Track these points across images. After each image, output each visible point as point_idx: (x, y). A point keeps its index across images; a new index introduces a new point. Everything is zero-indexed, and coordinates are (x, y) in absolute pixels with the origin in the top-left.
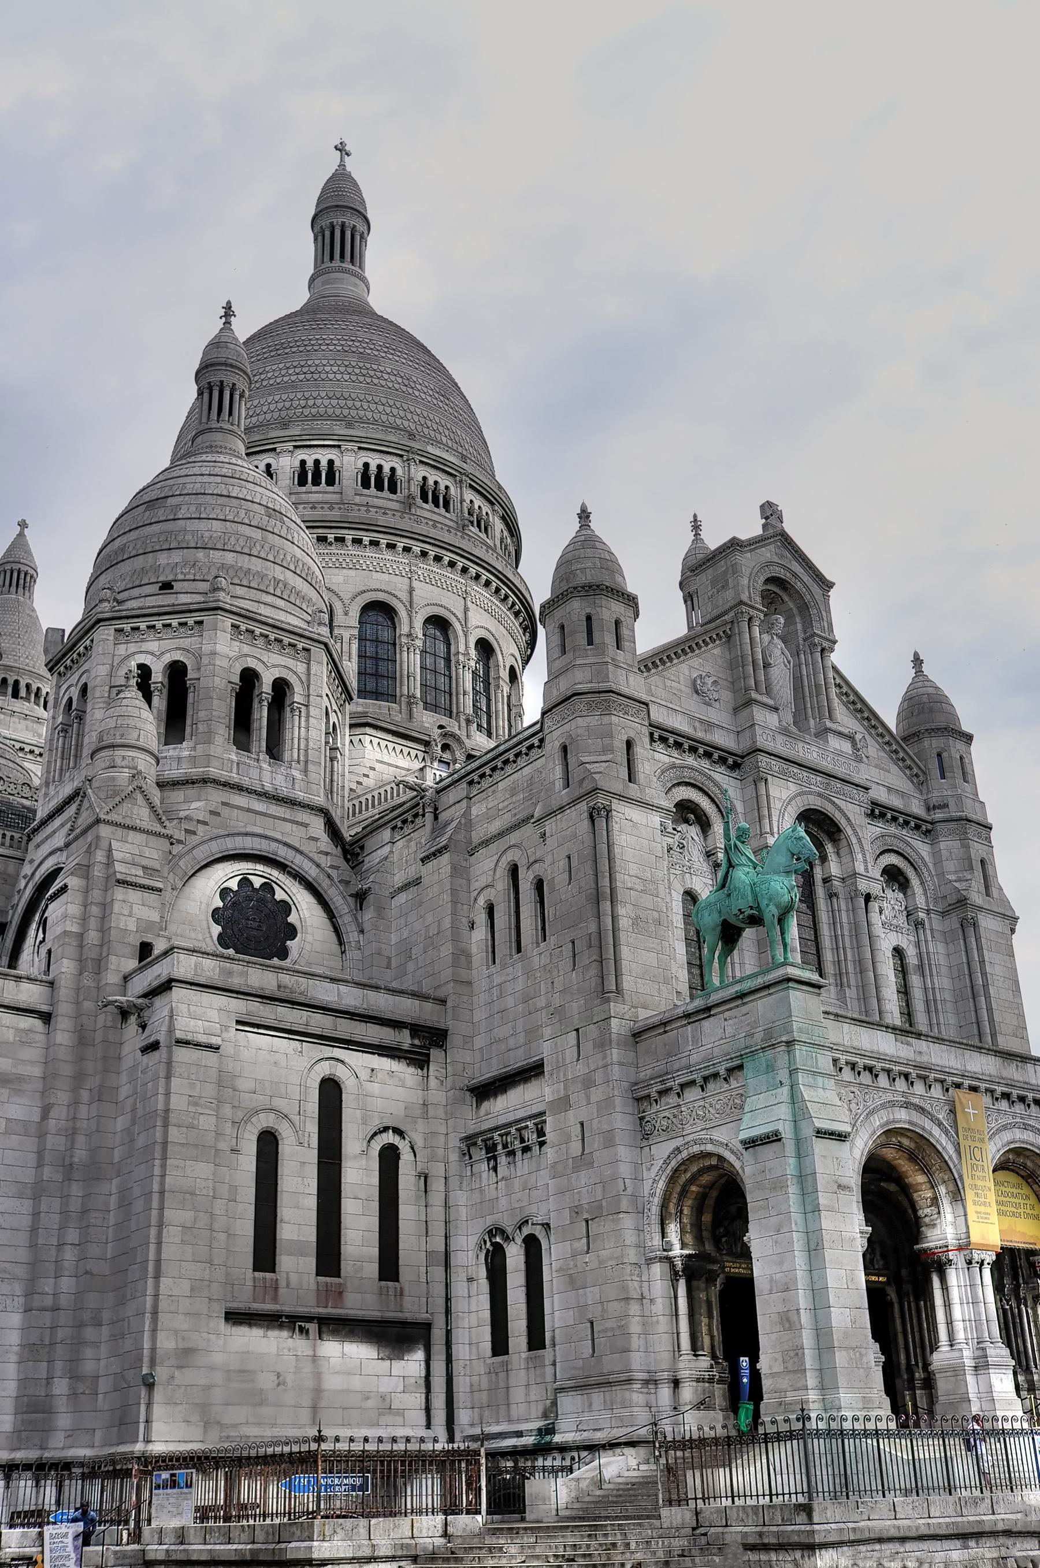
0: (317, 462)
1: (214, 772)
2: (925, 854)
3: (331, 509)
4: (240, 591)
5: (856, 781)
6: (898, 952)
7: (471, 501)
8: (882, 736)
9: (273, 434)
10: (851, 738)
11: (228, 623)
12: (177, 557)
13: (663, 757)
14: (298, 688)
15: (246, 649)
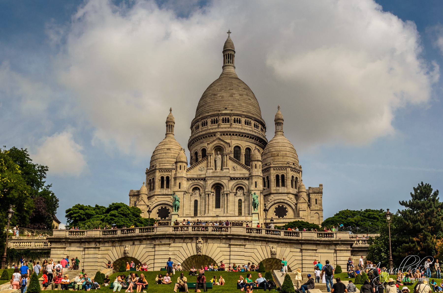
0: (204, 121)
1: (156, 193)
2: (246, 183)
3: (204, 131)
4: (162, 165)
5: (227, 176)
6: (240, 200)
7: (235, 118)
8: (241, 165)
9: (198, 118)
10: (229, 169)
11: (158, 171)
12: (154, 161)
13: (190, 182)
14: (170, 177)
15: (161, 174)
